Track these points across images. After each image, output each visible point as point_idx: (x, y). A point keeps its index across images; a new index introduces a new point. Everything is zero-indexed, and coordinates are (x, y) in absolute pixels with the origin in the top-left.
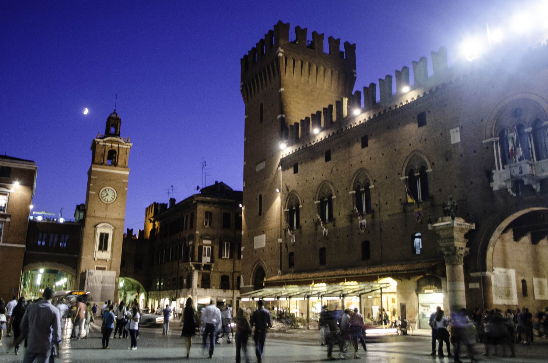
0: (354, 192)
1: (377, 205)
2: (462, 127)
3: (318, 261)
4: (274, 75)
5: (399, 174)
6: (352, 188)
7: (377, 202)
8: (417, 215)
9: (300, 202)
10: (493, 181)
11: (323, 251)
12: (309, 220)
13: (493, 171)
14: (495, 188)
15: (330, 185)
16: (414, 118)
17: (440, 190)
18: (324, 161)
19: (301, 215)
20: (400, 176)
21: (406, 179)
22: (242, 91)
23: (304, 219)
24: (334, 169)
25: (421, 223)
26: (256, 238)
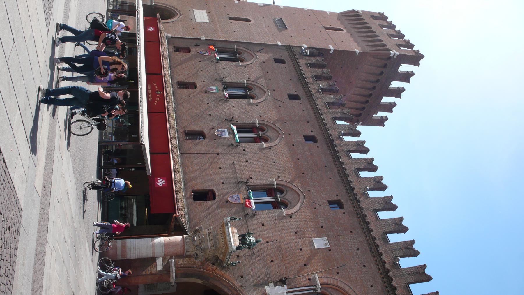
0: (258, 125)
1: (244, 150)
2: (330, 250)
3: (182, 79)
4: (372, 46)
5: (279, 177)
8: (235, 197)
9: (245, 64)
10: (275, 286)
11: (193, 86)
12: (225, 72)
13: (285, 286)
14: (267, 289)
15: (264, 98)
16: (337, 195)
17: (263, 225)
18: (288, 93)
19: (231, 63)
20: (277, 177)
21: (274, 185)
22: (353, 11)
23: (227, 66)
25: (227, 201)
26: (204, 12)
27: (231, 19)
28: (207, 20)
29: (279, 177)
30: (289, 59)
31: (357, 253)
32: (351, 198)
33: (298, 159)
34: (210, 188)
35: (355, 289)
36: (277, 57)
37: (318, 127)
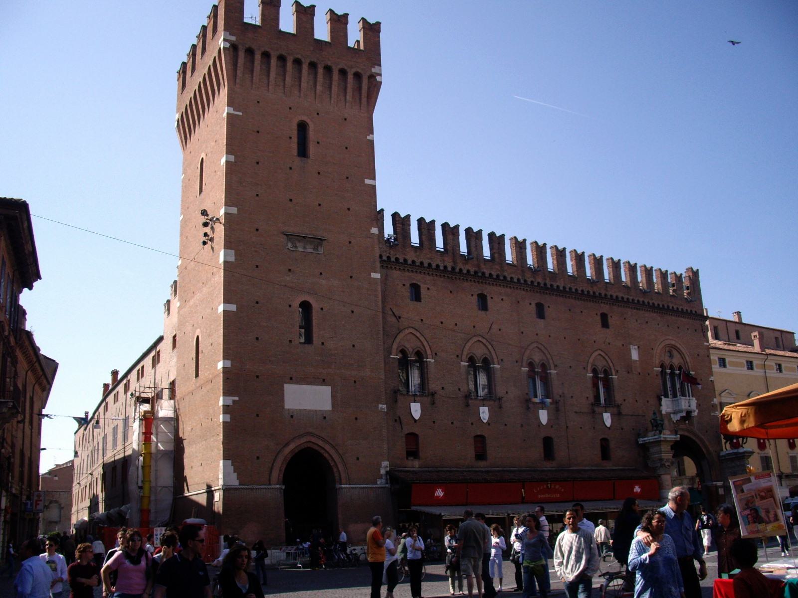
3: (471, 452)
6: (524, 363)
7: (561, 393)
14: (664, 412)
24: (495, 327)
27: (309, 340)
28: (326, 390)
29: (584, 368)
30: (407, 274)
31: (640, 324)
32: (600, 301)
33: (565, 338)
34: (599, 441)
35: (661, 340)
36: (406, 292)
37: (523, 292)
